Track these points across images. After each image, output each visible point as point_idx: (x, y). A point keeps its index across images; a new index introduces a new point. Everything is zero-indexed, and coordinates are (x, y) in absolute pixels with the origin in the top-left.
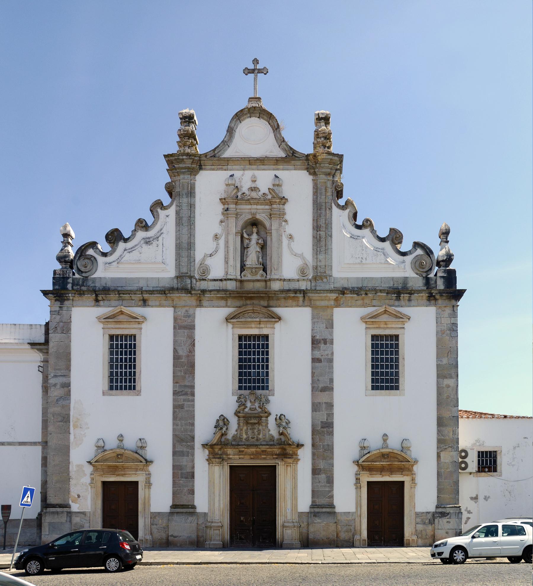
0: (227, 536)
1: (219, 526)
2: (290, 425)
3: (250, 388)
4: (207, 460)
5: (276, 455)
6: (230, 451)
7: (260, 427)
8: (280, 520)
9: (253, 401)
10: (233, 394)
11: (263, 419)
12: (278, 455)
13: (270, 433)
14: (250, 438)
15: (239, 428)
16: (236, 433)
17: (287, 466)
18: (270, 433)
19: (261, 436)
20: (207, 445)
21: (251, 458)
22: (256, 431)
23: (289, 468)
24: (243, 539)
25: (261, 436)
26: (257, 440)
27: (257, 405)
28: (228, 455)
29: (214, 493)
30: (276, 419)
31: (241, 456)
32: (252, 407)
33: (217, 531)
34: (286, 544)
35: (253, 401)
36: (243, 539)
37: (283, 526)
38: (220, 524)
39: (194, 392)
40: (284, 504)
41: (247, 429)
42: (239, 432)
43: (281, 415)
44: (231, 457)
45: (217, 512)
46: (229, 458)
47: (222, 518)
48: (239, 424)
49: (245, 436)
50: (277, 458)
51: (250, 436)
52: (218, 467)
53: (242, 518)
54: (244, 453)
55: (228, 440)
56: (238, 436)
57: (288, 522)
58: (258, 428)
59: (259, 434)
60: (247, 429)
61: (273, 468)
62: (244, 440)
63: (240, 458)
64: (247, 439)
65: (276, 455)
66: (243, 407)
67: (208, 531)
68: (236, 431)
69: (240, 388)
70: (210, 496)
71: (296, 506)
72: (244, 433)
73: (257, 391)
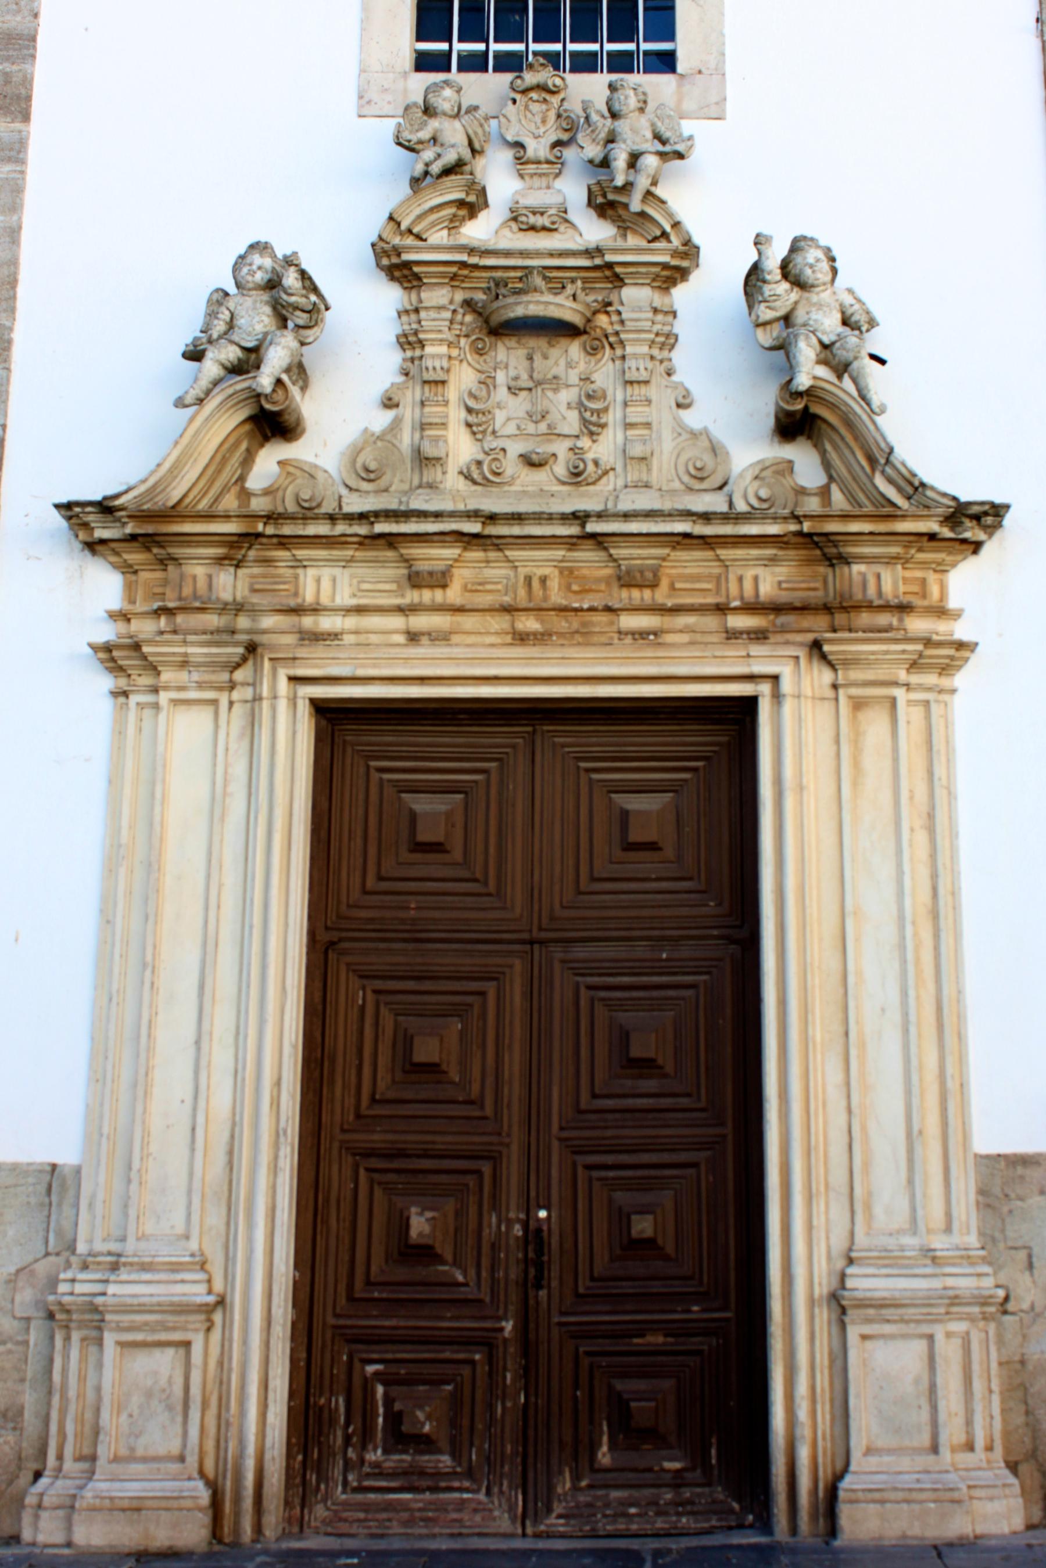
0: (264, 1421)
1: (182, 1309)
2: (876, 342)
3: (509, 63)
4: (108, 655)
5: (752, 608)
6: (330, 582)
7: (605, 373)
8: (802, 1247)
9: (537, 148)
10: (365, 106)
11: (629, 293)
12: (777, 608)
13: (692, 418)
14: (511, 466)
15: (419, 375)
16: (380, 420)
17: (858, 705)
18: (692, 418)
19: (604, 449)
20: (105, 508)
21: (522, 638)
22: (566, 396)
23: (875, 726)
24: (425, 1443)
25: (604, 449)
26: (576, 476)
27: (572, 190)
28: (297, 611)
29: (148, 966)
30: (754, 277)
31: (420, 622)
32: (535, 199)
33: (165, 1361)
34: (878, 1496)
35: (537, 148)
36: (425, 1443)
37: (839, 1304)
38: (196, 1292)
39: (27, 82)
40: (834, 1076)
41: (487, 382)
42: (409, 413)
43: (796, 246)
44: (327, 623)
45: (168, 1161)
46: (316, 637)
47: (216, 1219)
48: (410, 342)
49: (460, 448)
50: (759, 636)
51: (515, 449)
52: (202, 717)
53: (419, 1225)
54: (453, 594)
55: (311, 474)
56: (406, 439)
57: (890, 1260)
58: (586, 379)
59: (592, 428)
60: (487, 382)
61: (733, 720)
62: (453, 481)
63: (413, 637)
64: (482, 475)
65: (752, 608)
66: (452, 191)
67: (71, 1358)
68: (389, 403)
69: (424, 63)
70: (106, 998)
71: (951, 1095)
72: (456, 415)
73: (571, 78)
